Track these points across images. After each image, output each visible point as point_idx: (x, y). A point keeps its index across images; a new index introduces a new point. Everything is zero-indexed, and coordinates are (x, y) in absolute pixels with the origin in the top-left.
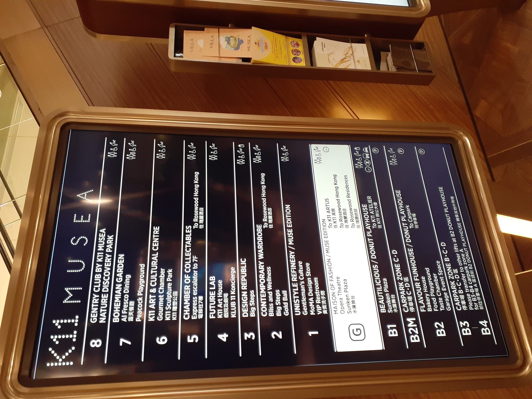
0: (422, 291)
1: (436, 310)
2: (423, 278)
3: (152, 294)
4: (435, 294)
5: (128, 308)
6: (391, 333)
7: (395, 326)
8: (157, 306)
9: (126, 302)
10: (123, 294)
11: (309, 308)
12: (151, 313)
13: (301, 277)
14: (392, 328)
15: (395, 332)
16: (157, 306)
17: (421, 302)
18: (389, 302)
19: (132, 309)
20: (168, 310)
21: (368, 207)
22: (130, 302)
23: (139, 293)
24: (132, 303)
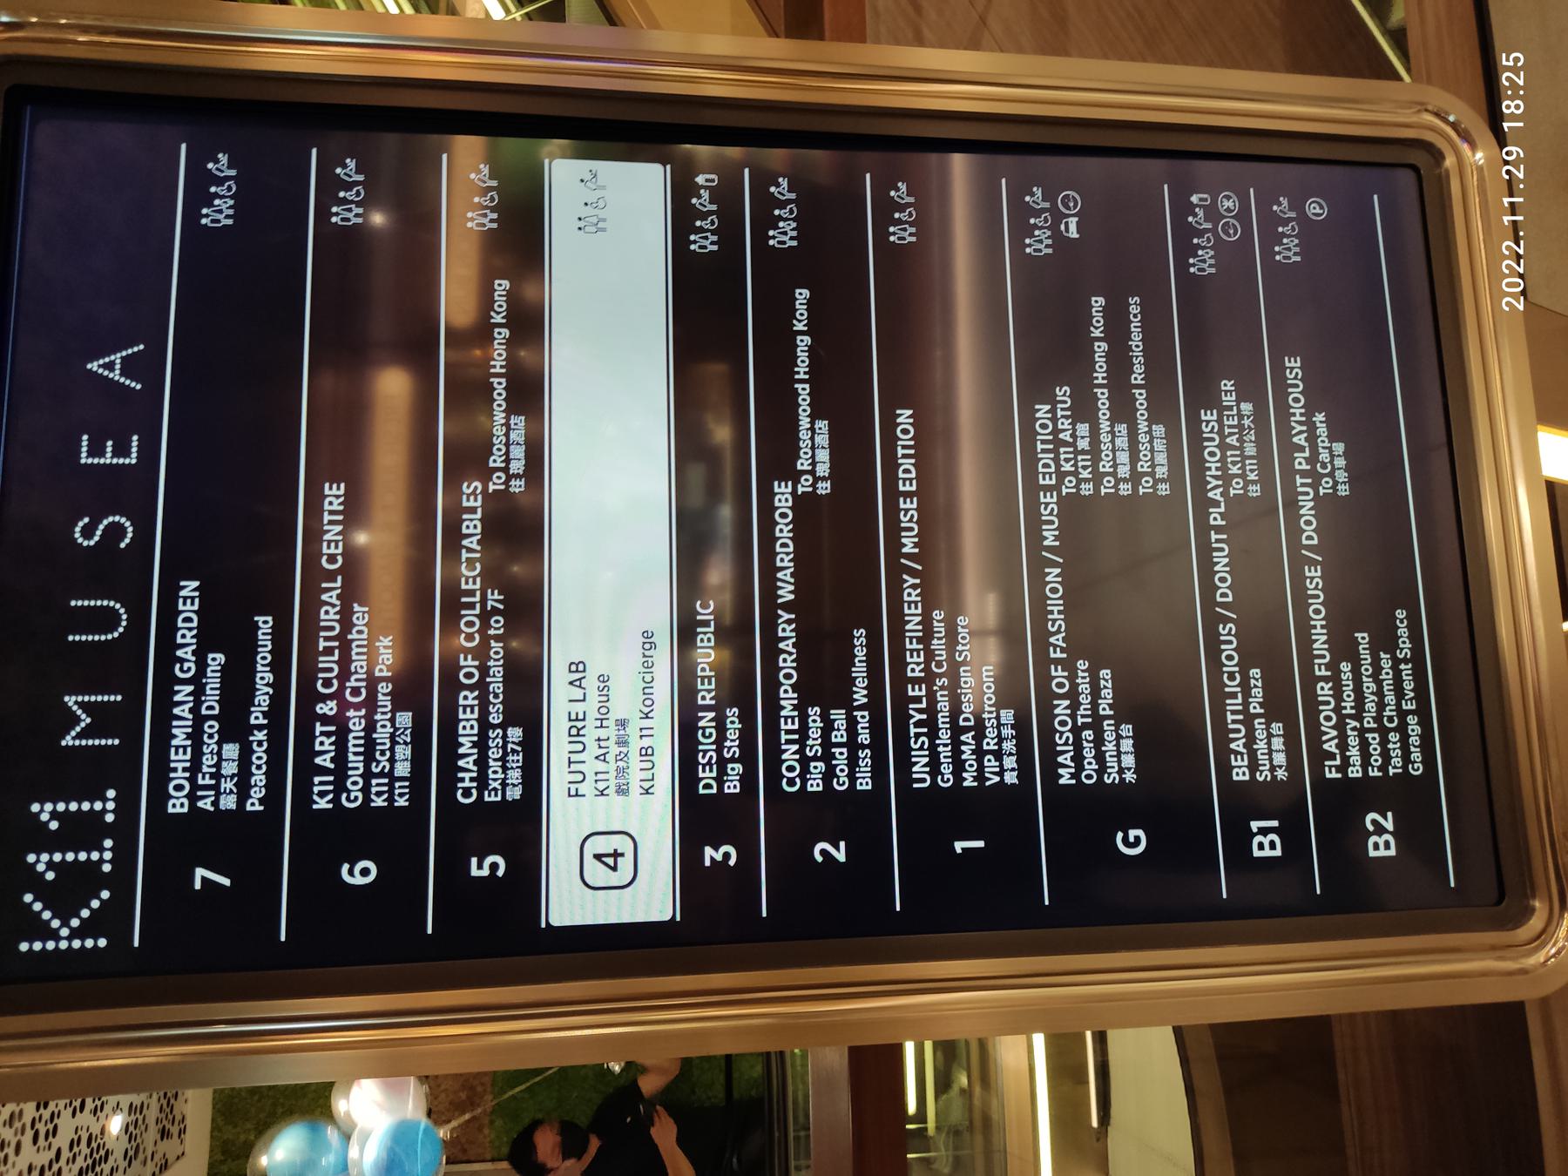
0: (1338, 709)
1: (1377, 774)
2: (1345, 667)
3: (325, 720)
4: (1378, 719)
5: (218, 765)
6: (1261, 847)
7: (1275, 823)
8: (341, 757)
9: (210, 745)
10: (199, 720)
11: (959, 766)
12: (321, 783)
13: (939, 665)
14: (1264, 831)
15: (1272, 845)
16: (341, 757)
17: (1331, 747)
18: (1261, 746)
19: (230, 768)
20: (381, 775)
21: (1220, 421)
22: (226, 747)
23: (257, 718)
24: (232, 751)
